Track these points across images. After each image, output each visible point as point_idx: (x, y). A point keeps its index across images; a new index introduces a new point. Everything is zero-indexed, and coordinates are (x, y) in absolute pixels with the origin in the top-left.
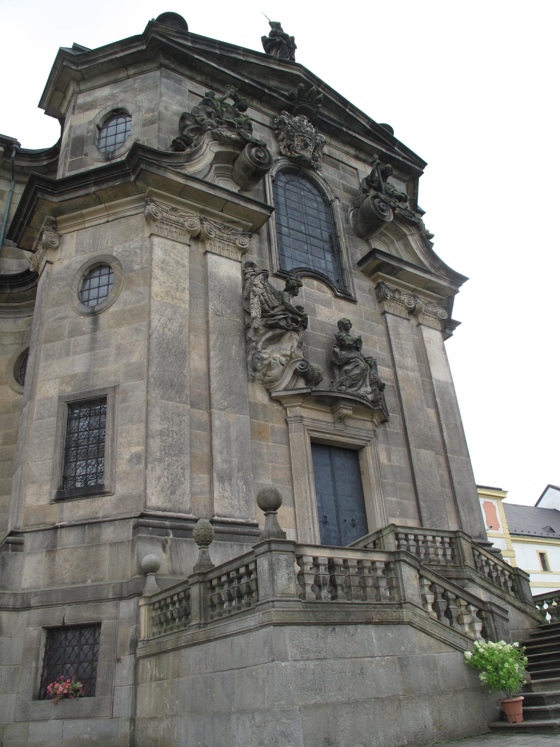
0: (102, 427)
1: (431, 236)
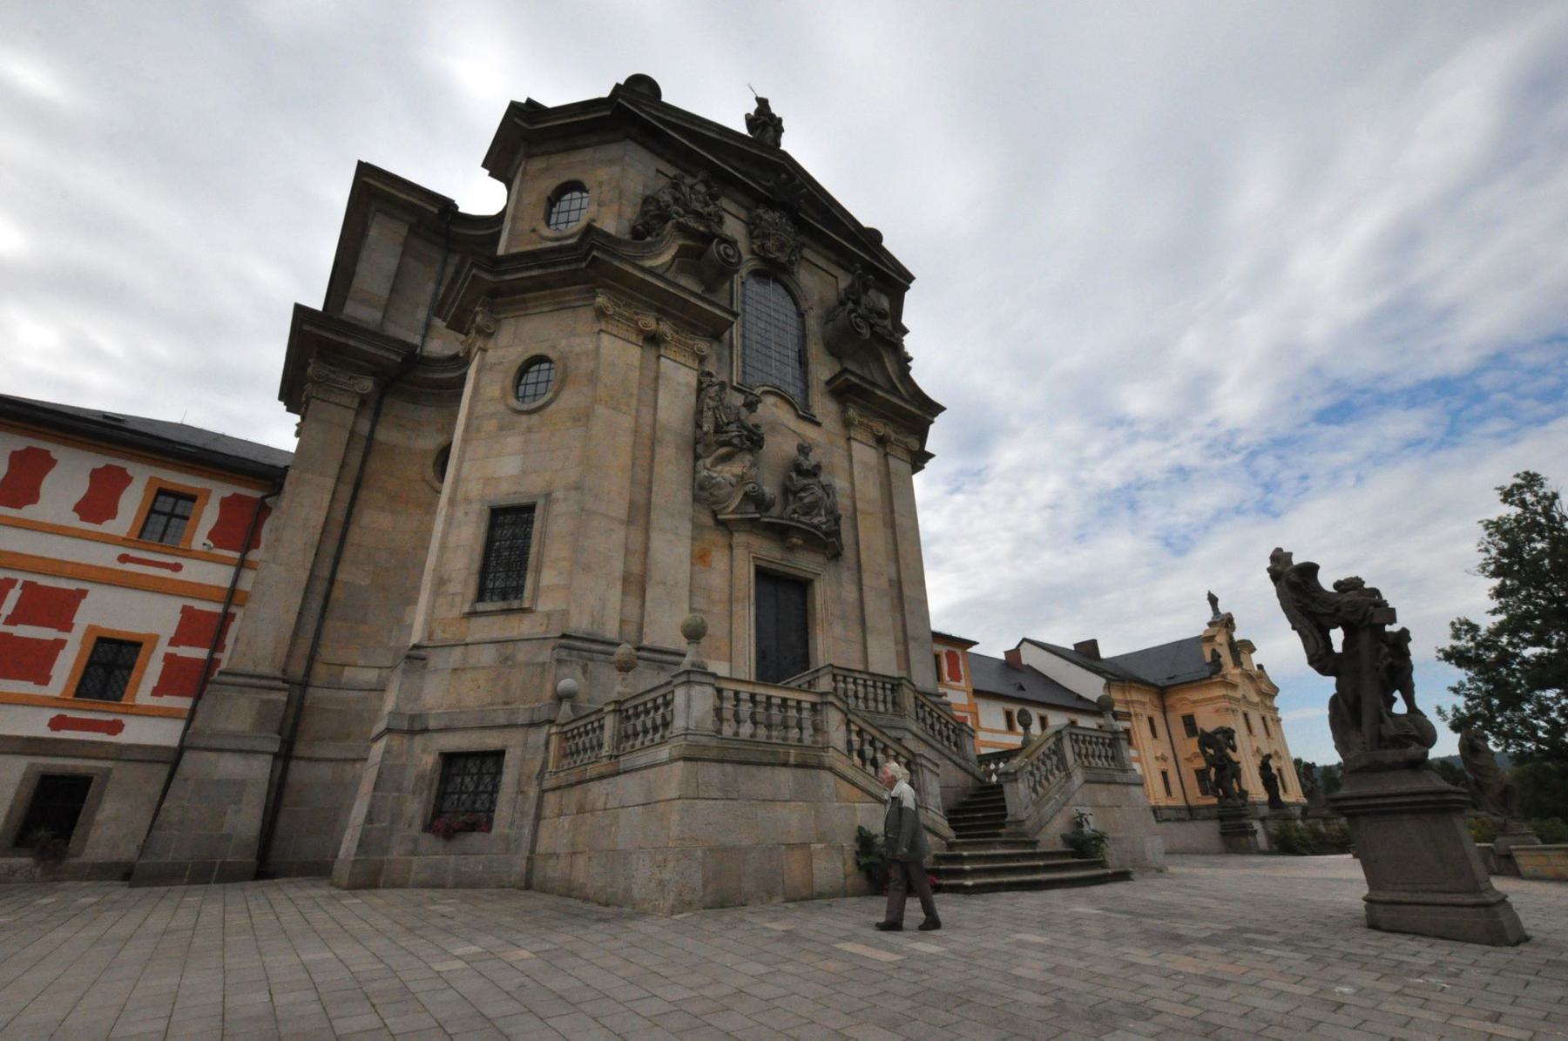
0: (527, 537)
1: (910, 359)
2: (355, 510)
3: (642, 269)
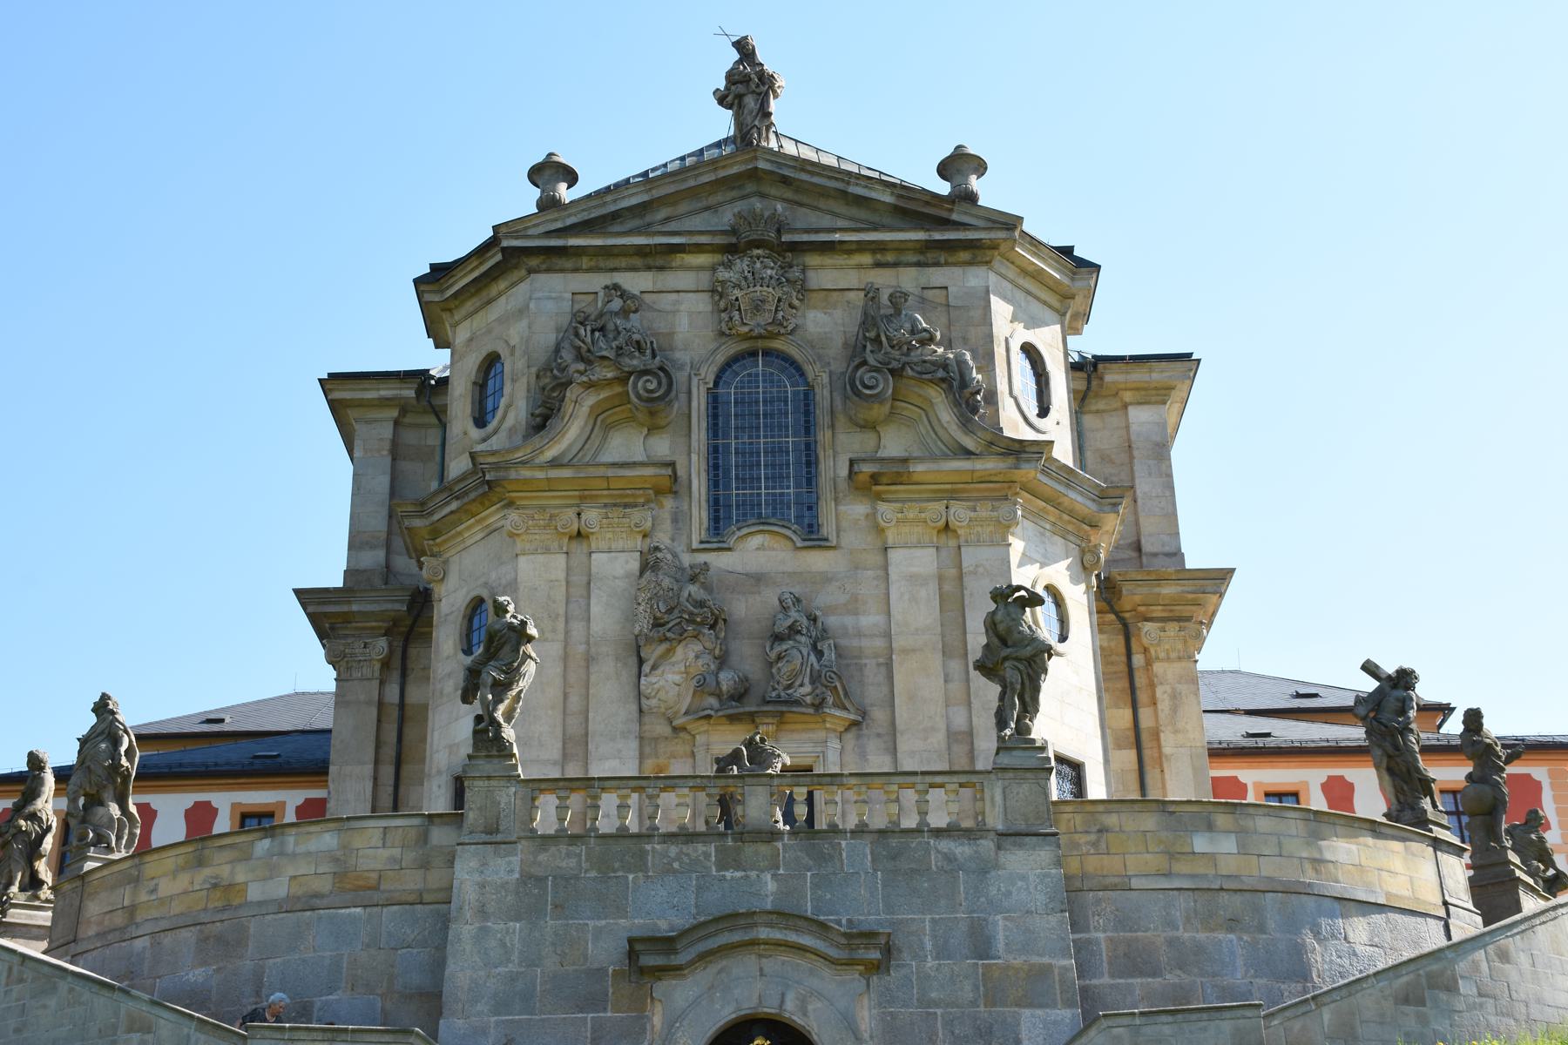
2: (402, 790)
3: (541, 467)
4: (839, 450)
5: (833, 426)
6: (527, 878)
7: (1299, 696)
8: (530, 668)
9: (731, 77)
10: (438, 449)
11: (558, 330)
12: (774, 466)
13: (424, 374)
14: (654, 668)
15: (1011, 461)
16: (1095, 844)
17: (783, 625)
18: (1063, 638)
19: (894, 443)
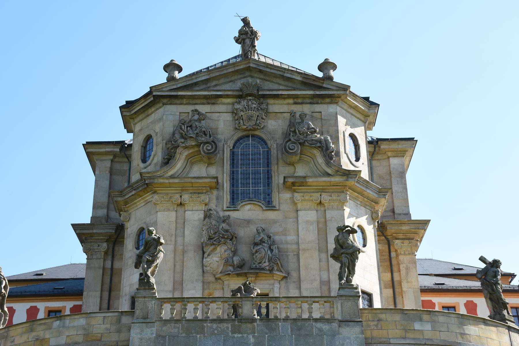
2: (111, 302)
3: (167, 178)
4: (280, 173)
5: (277, 164)
6: (158, 336)
7: (455, 269)
8: (161, 255)
9: (240, 32)
10: (128, 171)
11: (174, 126)
12: (255, 179)
13: (122, 143)
14: (209, 255)
15: (345, 178)
16: (376, 326)
17: (258, 240)
18: (364, 246)
19: (301, 171)
